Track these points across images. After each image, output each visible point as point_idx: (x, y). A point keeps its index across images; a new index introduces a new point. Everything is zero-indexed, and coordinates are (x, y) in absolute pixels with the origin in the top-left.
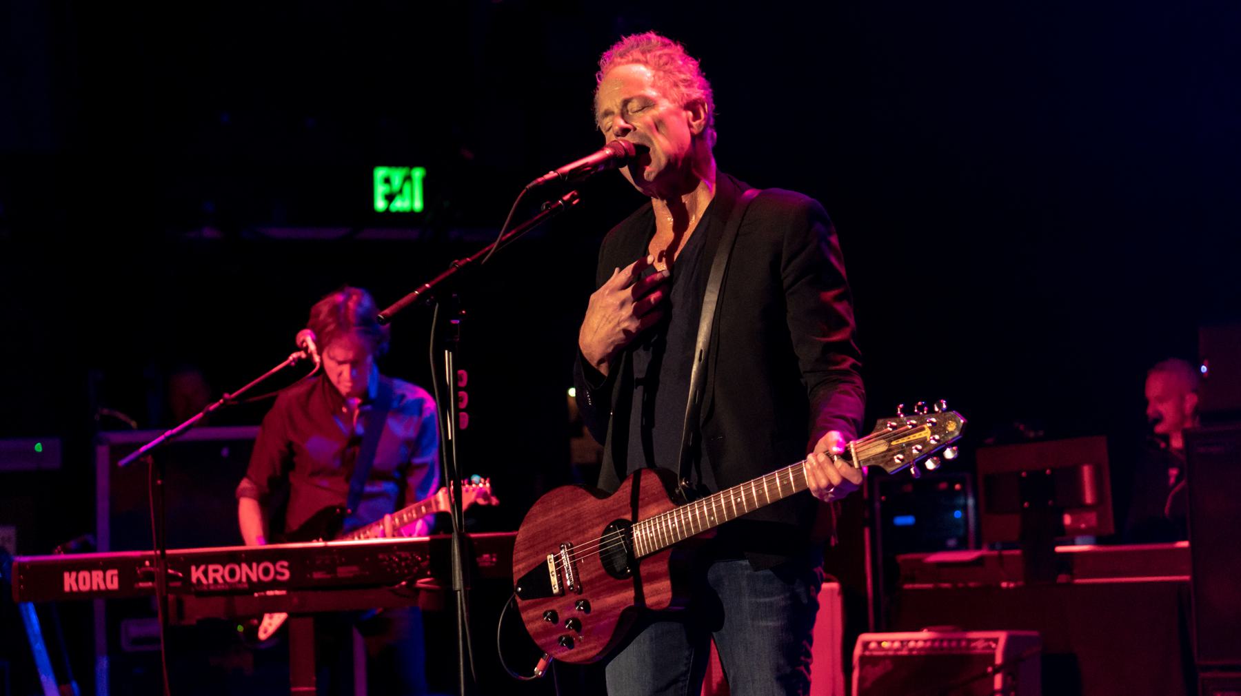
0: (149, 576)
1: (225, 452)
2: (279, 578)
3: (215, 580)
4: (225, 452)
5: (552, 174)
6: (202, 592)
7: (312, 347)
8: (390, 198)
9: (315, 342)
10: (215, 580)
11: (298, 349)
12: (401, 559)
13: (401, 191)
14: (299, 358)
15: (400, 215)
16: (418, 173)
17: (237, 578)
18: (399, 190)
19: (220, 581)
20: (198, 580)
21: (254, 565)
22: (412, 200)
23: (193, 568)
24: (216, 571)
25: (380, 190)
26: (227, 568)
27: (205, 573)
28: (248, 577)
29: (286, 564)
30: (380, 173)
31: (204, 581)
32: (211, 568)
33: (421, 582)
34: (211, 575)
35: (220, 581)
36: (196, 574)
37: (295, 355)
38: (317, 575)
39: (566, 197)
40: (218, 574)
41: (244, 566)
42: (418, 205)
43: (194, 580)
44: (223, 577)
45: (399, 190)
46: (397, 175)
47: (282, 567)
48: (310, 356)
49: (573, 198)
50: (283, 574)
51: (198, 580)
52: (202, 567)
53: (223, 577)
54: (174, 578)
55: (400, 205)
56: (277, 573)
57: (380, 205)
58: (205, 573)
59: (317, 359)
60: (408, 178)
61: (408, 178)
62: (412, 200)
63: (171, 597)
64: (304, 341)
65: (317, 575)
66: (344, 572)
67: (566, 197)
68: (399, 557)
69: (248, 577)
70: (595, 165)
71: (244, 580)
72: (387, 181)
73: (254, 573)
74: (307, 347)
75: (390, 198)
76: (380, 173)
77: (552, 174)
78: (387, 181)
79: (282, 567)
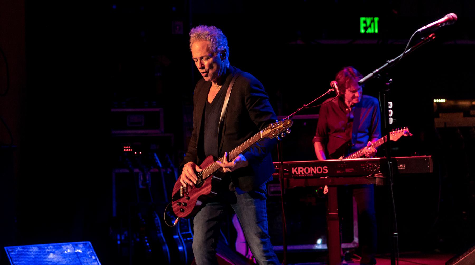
0: (277, 171)
1: (305, 124)
2: (324, 172)
3: (301, 172)
4: (305, 124)
5: (424, 28)
6: (296, 177)
7: (336, 87)
8: (366, 28)
9: (337, 85)
10: (301, 172)
11: (331, 88)
12: (369, 166)
13: (370, 26)
14: (332, 91)
15: (370, 34)
16: (376, 19)
17: (309, 172)
18: (369, 25)
19: (303, 173)
20: (295, 172)
21: (315, 167)
22: (374, 29)
23: (293, 168)
24: (301, 169)
25: (362, 25)
26: (305, 169)
27: (297, 170)
28: (313, 171)
29: (327, 167)
30: (362, 19)
31: (297, 173)
32: (299, 168)
33: (377, 175)
34: (299, 171)
35: (303, 173)
36: (294, 171)
37: (330, 90)
38: (338, 172)
39: (430, 36)
40: (302, 171)
41: (311, 168)
42: (376, 31)
43: (293, 173)
44: (304, 172)
45: (369, 25)
46: (369, 20)
47: (325, 168)
48: (335, 90)
49: (433, 36)
50: (326, 171)
51: (295, 172)
52: (296, 168)
53: (304, 172)
54: (286, 172)
55: (370, 31)
56: (323, 171)
57: (362, 31)
58: (297, 170)
59: (338, 91)
60: (373, 21)
61: (373, 21)
62: (374, 29)
63: (285, 179)
64: (333, 85)
65: (338, 172)
66: (348, 170)
67: (430, 36)
68: (368, 165)
69: (313, 171)
70: (441, 23)
71: (311, 173)
72: (365, 22)
73: (316, 171)
74: (334, 87)
75: (366, 28)
76: (362, 19)
77: (424, 28)
78: (365, 22)
79: (325, 168)
